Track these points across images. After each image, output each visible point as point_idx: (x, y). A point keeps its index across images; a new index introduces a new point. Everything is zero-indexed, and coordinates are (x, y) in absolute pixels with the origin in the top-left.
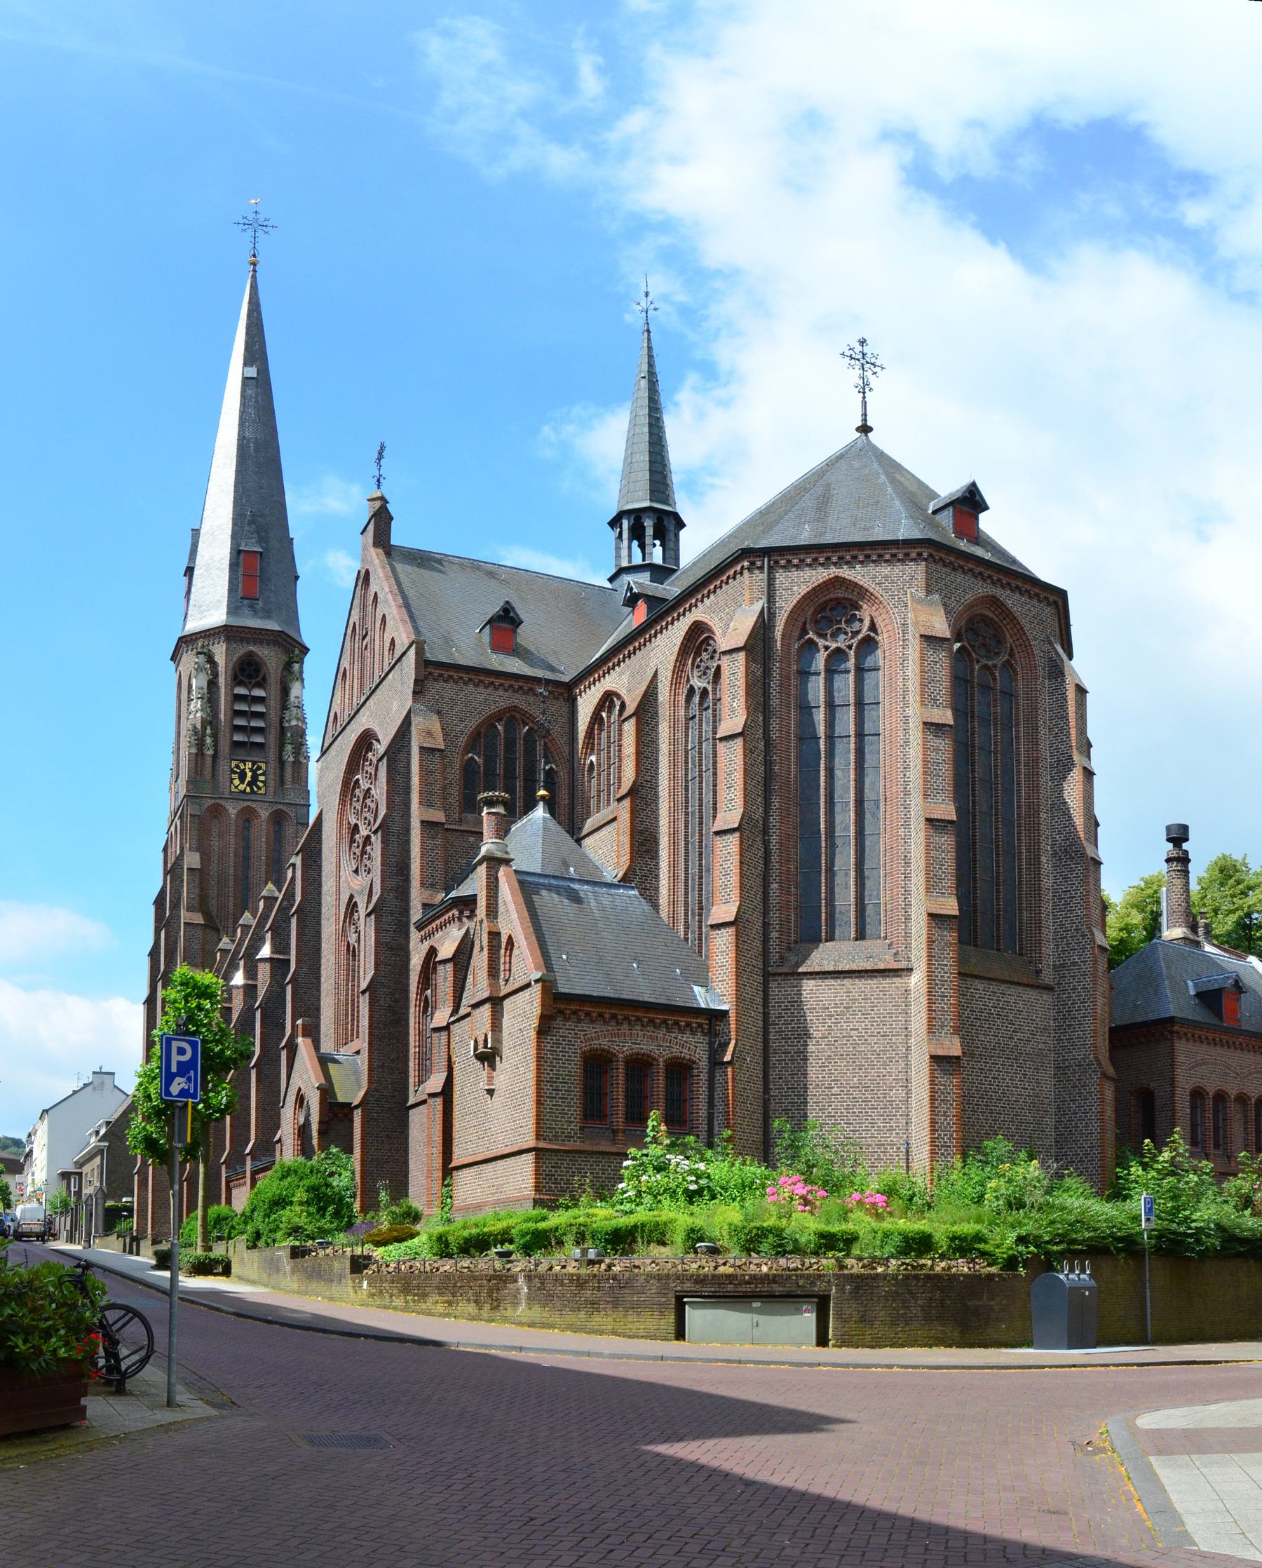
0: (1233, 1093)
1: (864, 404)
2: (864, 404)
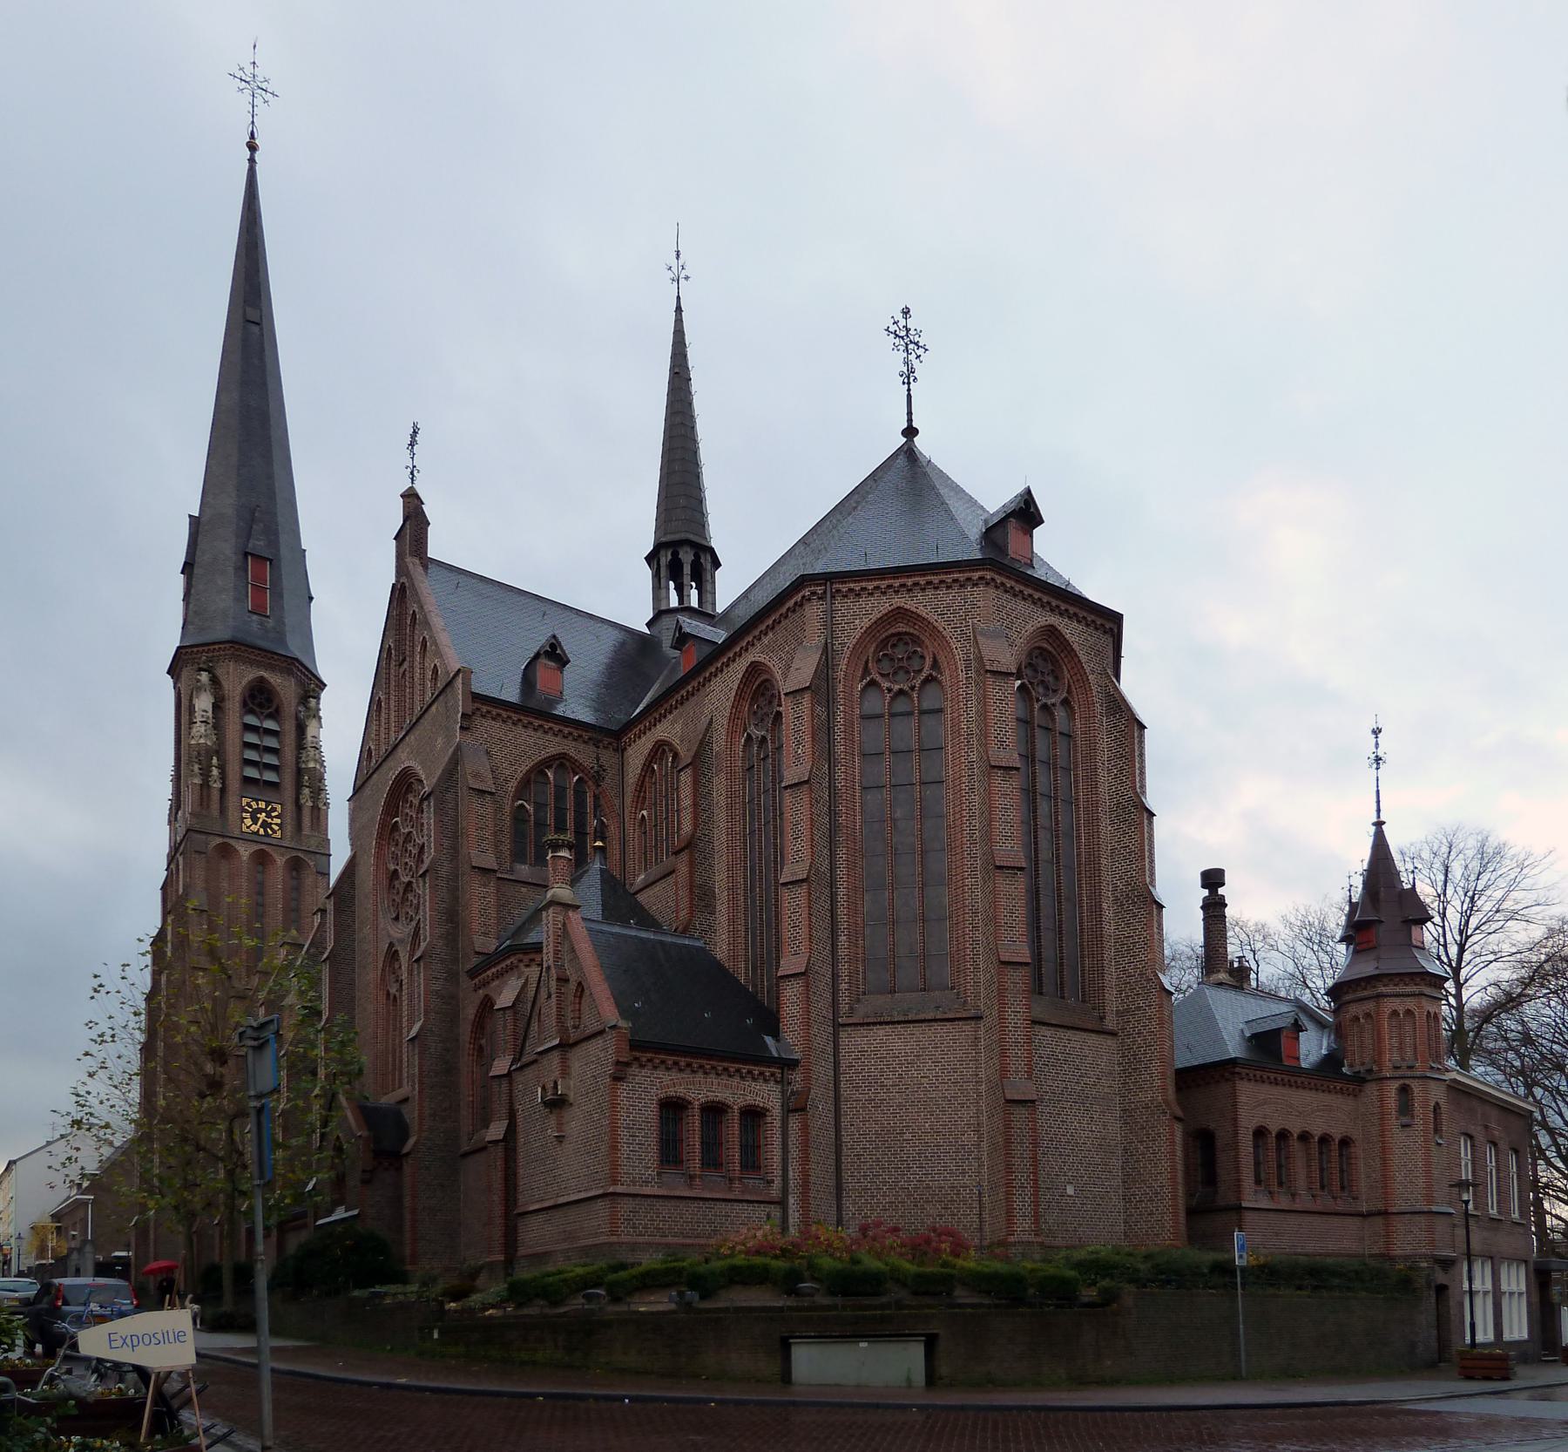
0: (1296, 1131)
1: (909, 397)
2: (909, 397)
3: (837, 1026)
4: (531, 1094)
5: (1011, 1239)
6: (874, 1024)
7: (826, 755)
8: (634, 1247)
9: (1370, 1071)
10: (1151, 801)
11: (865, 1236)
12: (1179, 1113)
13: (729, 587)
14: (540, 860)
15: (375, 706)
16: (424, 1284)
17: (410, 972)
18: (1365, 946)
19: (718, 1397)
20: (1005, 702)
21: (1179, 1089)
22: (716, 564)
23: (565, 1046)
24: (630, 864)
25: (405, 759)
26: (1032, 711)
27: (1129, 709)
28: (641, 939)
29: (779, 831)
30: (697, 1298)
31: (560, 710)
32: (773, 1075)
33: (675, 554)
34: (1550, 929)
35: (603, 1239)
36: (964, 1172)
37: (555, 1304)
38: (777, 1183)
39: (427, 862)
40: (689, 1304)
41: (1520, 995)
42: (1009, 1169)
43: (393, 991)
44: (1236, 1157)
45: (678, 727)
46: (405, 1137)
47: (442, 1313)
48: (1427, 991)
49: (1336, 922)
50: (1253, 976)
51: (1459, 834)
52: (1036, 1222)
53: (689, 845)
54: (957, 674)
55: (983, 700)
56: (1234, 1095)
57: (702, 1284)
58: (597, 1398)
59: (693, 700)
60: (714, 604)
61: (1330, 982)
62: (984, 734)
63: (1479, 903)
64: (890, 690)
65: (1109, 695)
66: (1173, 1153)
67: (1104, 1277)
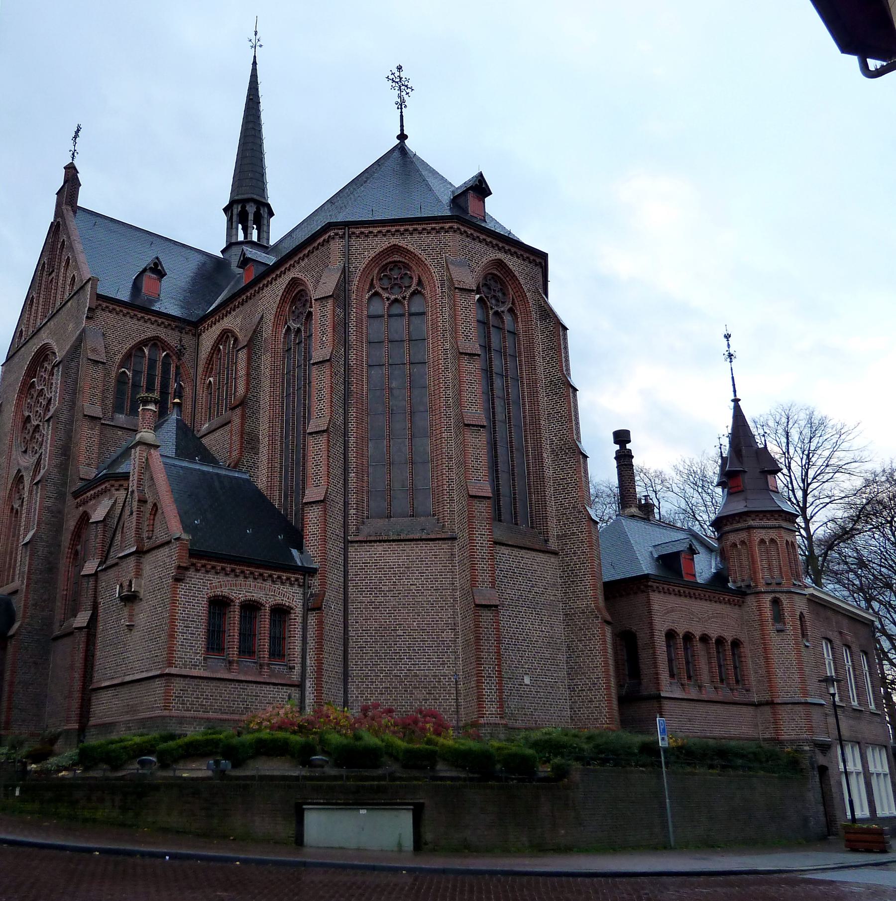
0: (698, 634)
1: (402, 116)
2: (402, 116)
3: (347, 543)
4: (111, 590)
5: (482, 721)
6: (375, 541)
7: (342, 342)
8: (181, 720)
9: (749, 586)
10: (575, 380)
11: (365, 716)
12: (609, 618)
13: (279, 229)
14: (134, 411)
15: (29, 301)
16: (13, 747)
17: (31, 492)
18: (736, 489)
19: (242, 856)
20: (469, 310)
21: (607, 598)
22: (271, 214)
23: (140, 553)
24: (198, 416)
25: (45, 338)
26: (488, 316)
27: (556, 316)
28: (203, 472)
29: (307, 395)
30: (230, 766)
31: (156, 307)
32: (297, 580)
33: (243, 208)
34: (866, 480)
35: (158, 713)
36: (443, 664)
37: (115, 768)
38: (298, 668)
39: (52, 410)
40: (223, 771)
41: (852, 529)
42: (479, 661)
43: (16, 506)
44: (654, 653)
45: (239, 320)
46: (11, 621)
47: (25, 772)
48: (784, 524)
49: (713, 471)
50: (656, 510)
51: (793, 409)
52: (501, 707)
53: (242, 403)
54: (435, 291)
55: (453, 307)
56: (648, 603)
57: (235, 754)
58: (143, 854)
59: (250, 302)
60: (268, 239)
61: (713, 517)
62: (454, 331)
63: (813, 459)
64: (388, 299)
65: (540, 306)
66: (605, 650)
67: (556, 756)
